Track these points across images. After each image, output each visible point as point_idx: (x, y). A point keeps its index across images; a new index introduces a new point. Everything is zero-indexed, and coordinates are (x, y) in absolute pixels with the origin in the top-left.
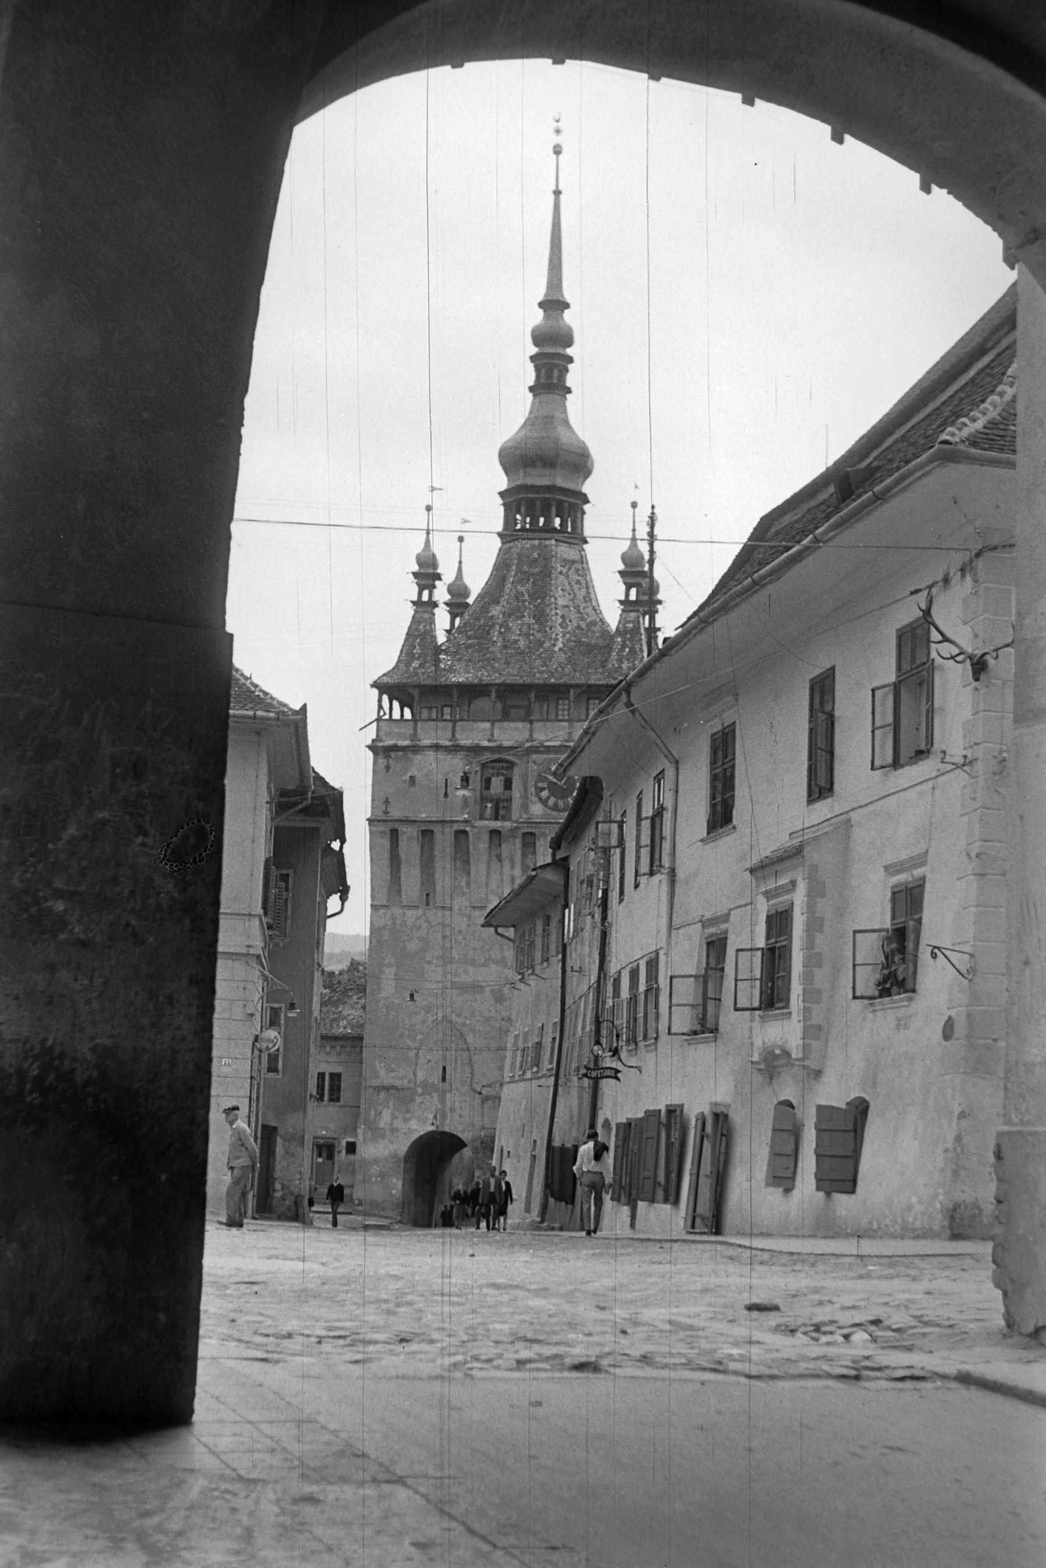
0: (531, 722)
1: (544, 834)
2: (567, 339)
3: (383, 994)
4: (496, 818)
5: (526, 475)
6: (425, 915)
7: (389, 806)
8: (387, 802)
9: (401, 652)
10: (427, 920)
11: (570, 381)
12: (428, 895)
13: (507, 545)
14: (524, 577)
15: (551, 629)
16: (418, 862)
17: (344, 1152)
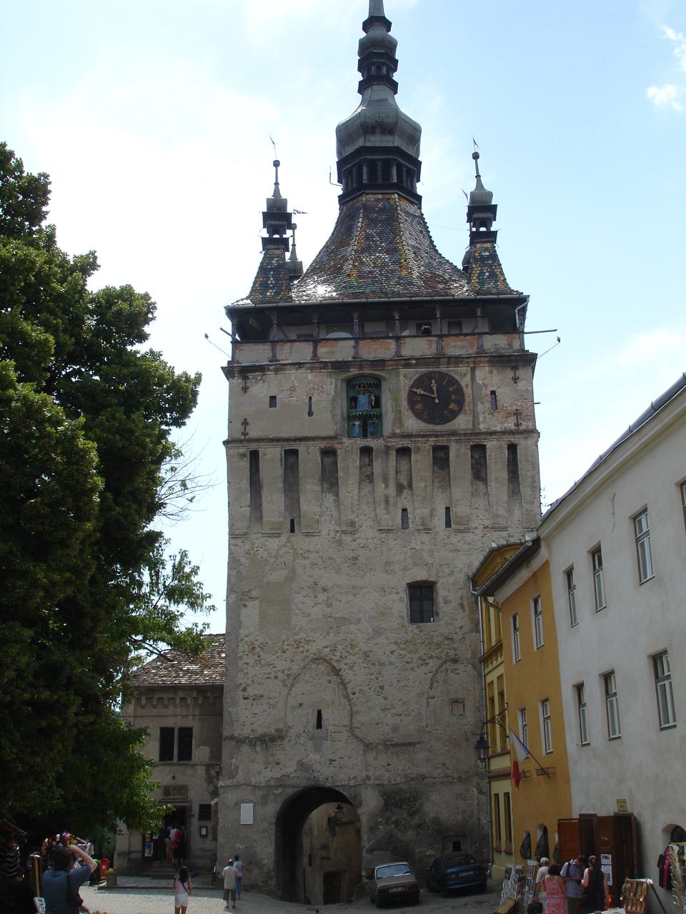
0: (398, 339)
1: (418, 450)
2: (391, 46)
3: (243, 632)
4: (365, 435)
5: (365, 141)
6: (290, 542)
7: (248, 427)
8: (245, 423)
9: (254, 283)
10: (292, 546)
11: (396, 77)
12: (292, 521)
13: (351, 203)
14: (371, 223)
15: (405, 261)
16: (281, 485)
17: (197, 816)
